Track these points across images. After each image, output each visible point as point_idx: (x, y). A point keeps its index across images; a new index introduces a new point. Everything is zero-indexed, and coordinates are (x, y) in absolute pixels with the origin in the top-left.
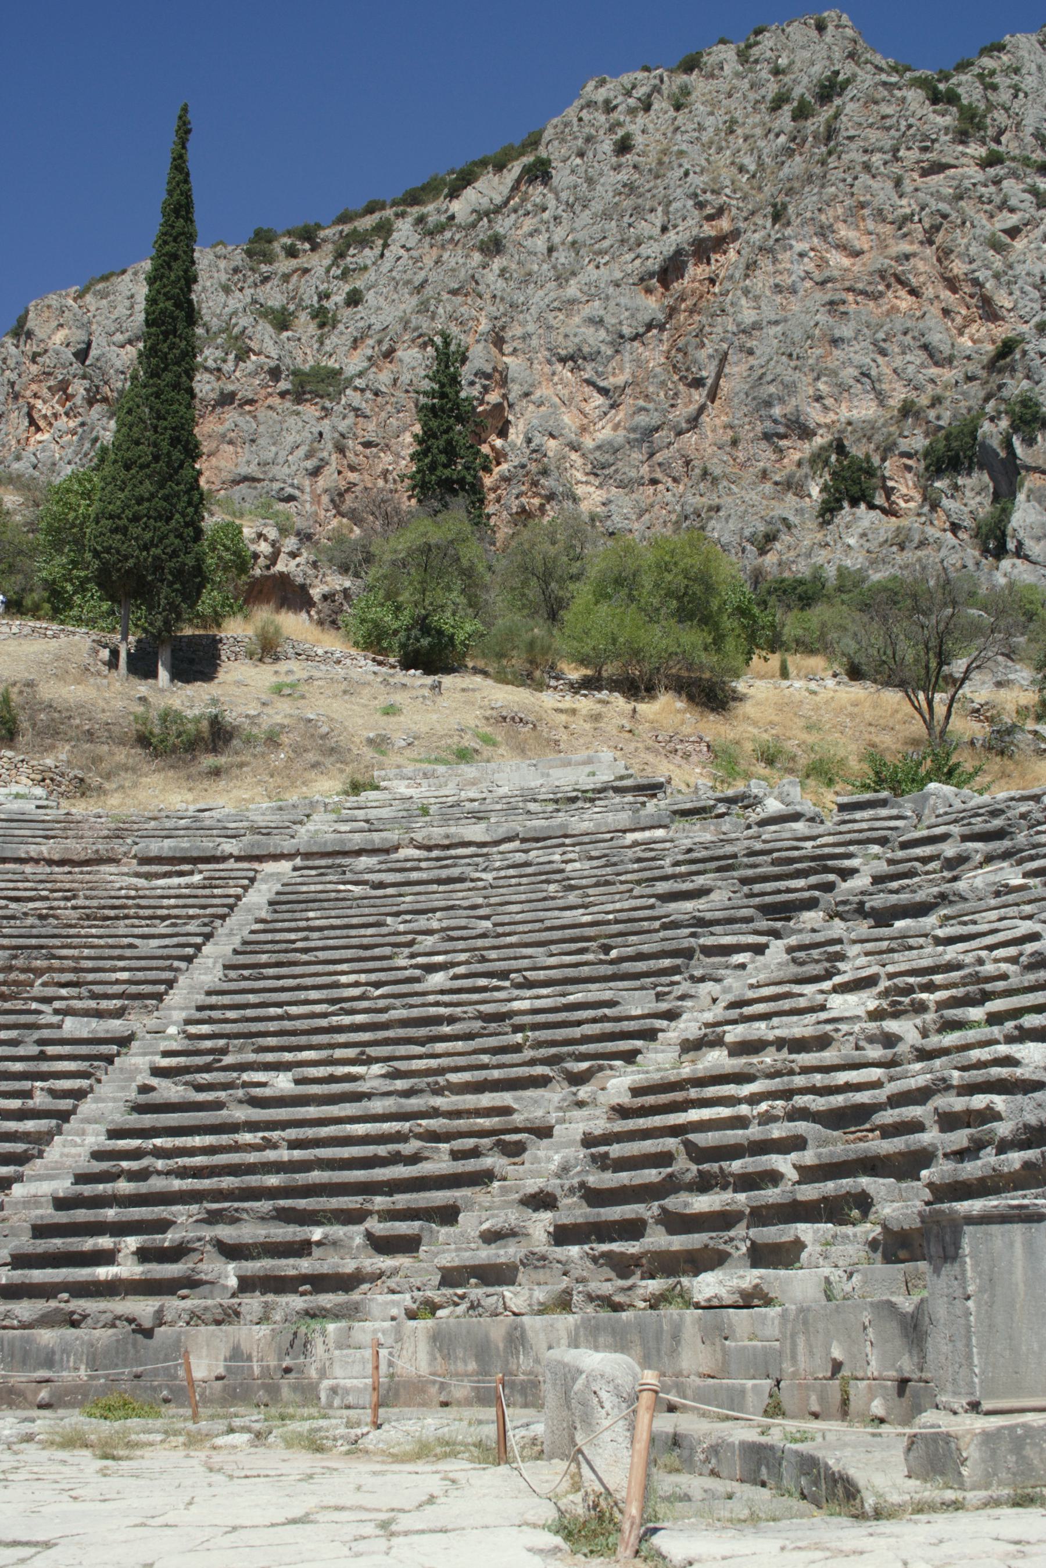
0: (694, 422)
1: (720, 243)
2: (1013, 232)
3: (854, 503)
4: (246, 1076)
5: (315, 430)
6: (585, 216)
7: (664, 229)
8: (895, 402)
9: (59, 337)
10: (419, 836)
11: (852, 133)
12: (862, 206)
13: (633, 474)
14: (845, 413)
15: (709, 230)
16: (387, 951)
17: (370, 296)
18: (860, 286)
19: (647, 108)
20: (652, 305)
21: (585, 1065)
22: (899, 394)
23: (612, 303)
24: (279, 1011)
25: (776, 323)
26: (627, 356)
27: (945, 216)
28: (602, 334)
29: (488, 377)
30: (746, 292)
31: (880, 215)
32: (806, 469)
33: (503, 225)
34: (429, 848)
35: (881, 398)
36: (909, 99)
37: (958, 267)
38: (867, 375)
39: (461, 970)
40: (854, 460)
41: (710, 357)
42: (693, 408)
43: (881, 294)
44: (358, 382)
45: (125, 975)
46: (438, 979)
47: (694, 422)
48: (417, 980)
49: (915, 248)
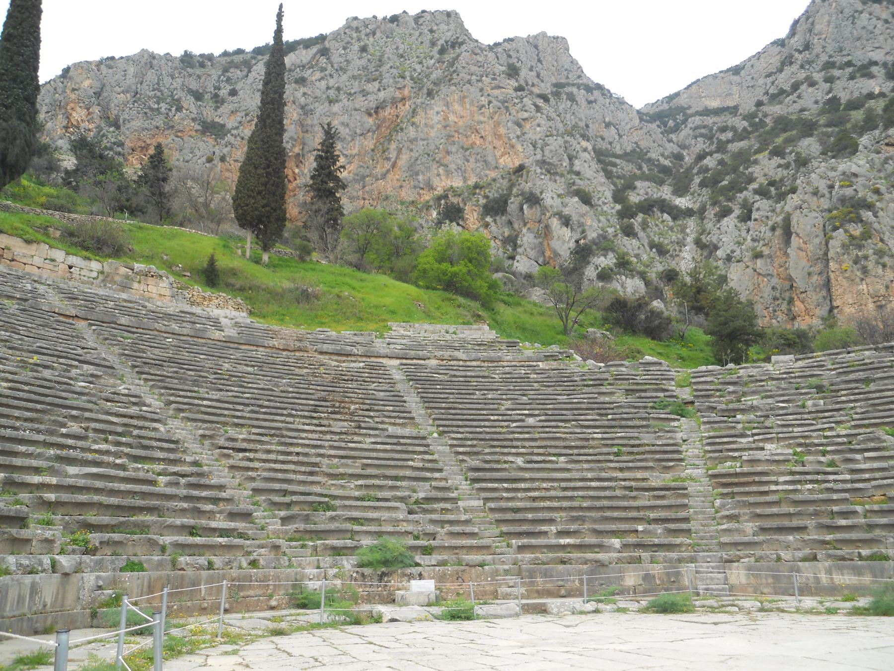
0: (384, 176)
3: (451, 221)
4: (506, 458)
5: (212, 150)
6: (344, 77)
7: (379, 90)
9: (87, 83)
11: (464, 65)
12: (464, 97)
13: (355, 194)
14: (449, 183)
15: (398, 95)
17: (241, 93)
18: (461, 131)
19: (374, 34)
20: (370, 121)
21: (671, 464)
23: (353, 118)
25: (424, 140)
26: (357, 143)
28: (347, 130)
29: (295, 140)
30: (413, 124)
33: (307, 74)
34: (442, 360)
35: (465, 179)
37: (502, 130)
39: (543, 418)
42: (384, 170)
44: (234, 132)
45: (391, 408)
46: (531, 421)
47: (384, 176)
48: (523, 421)
49: (485, 119)
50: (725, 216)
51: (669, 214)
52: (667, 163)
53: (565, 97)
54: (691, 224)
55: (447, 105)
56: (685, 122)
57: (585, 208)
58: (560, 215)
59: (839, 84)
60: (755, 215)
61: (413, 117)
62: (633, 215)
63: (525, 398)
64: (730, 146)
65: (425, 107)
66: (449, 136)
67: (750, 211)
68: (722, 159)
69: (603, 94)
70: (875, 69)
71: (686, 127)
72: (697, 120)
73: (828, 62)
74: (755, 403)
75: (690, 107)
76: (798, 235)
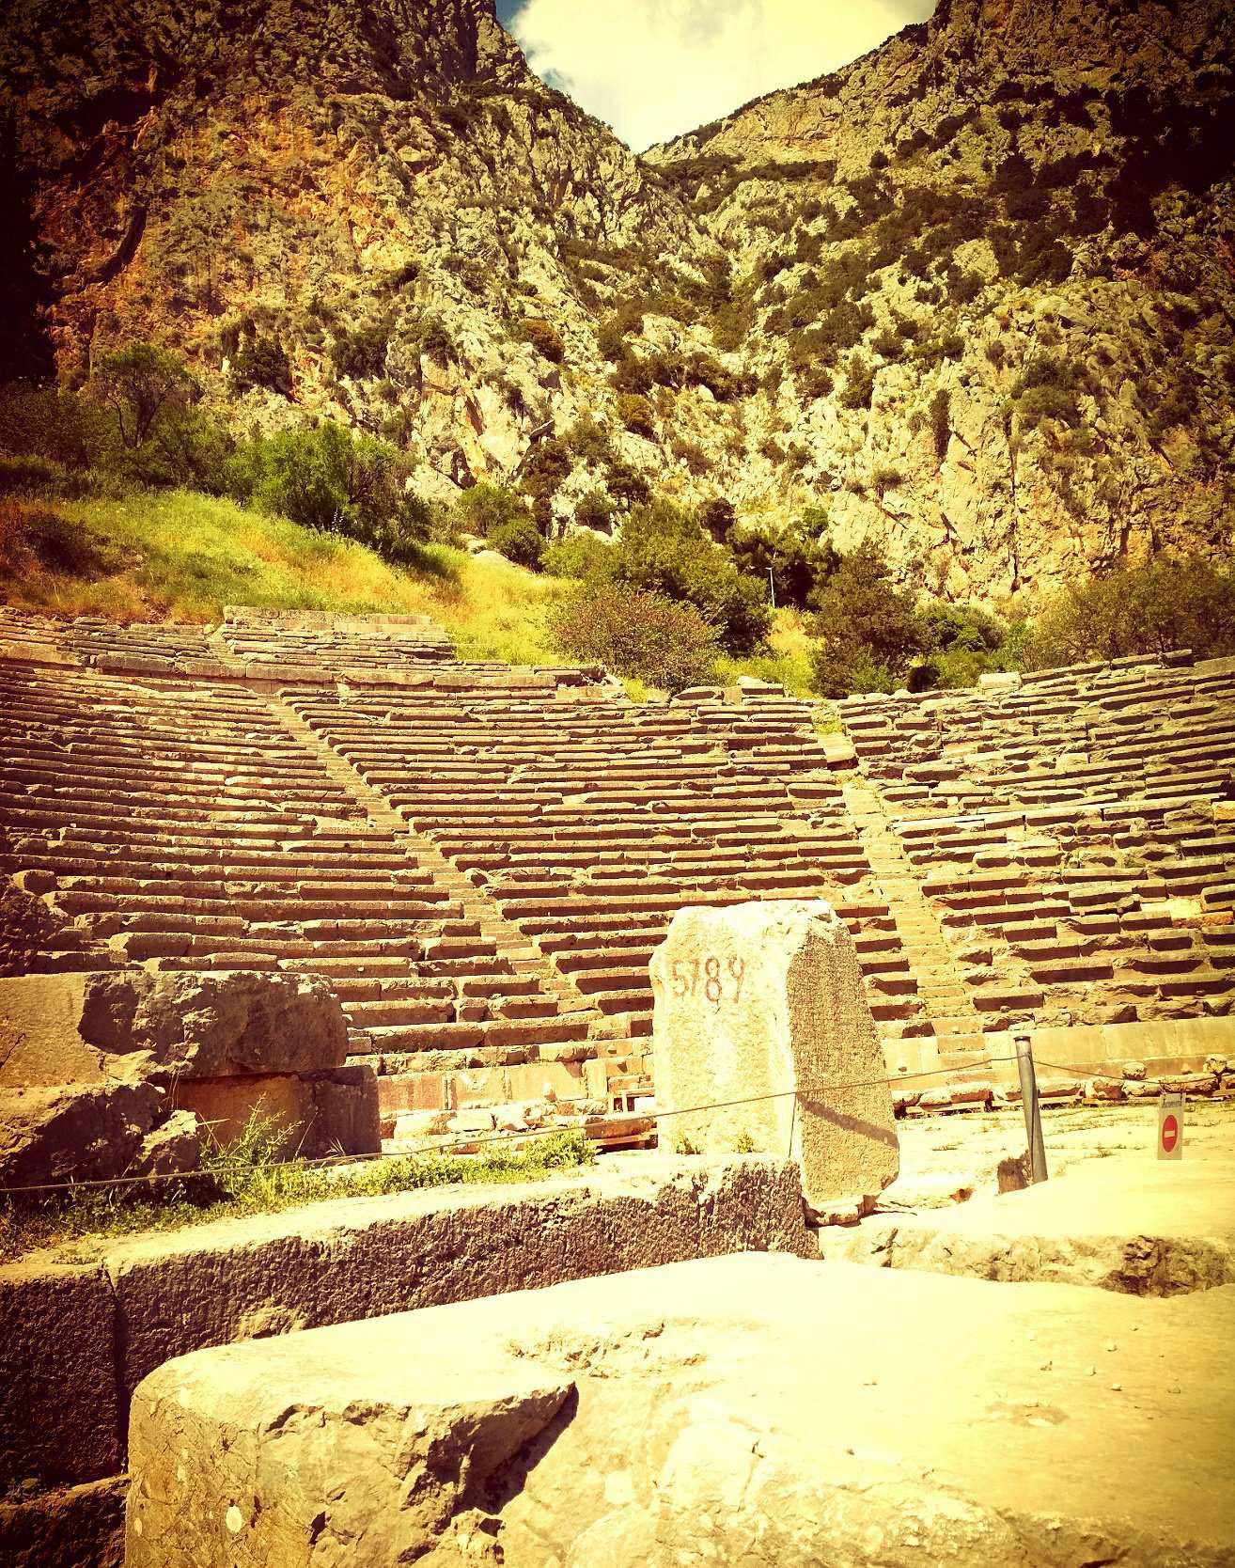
1: (145, 102)
2: (417, 167)
3: (263, 382)
4: (553, 870)
8: (305, 299)
10: (354, 673)
11: (278, 29)
14: (252, 299)
16: (501, 775)
18: (276, 180)
21: (852, 870)
22: (307, 294)
24: (491, 820)
25: (191, 195)
27: (359, 135)
31: (297, 118)
32: (216, 342)
35: (291, 293)
36: (332, 15)
38: (278, 267)
39: (595, 795)
40: (264, 342)
41: (126, 212)
42: (105, 259)
43: (296, 194)
46: (573, 802)
48: (559, 801)
49: (328, 157)
50: (818, 395)
51: (713, 388)
52: (697, 276)
53: (489, 120)
54: (754, 408)
55: (242, 118)
56: (730, 189)
57: (546, 367)
58: (495, 378)
59: (1027, 134)
60: (878, 396)
61: (167, 142)
62: (642, 387)
63: (547, 758)
64: (824, 246)
65: (192, 121)
66: (248, 192)
67: (868, 388)
68: (811, 275)
69: (569, 120)
70: (1093, 108)
71: (733, 200)
72: (755, 189)
73: (1006, 84)
74: (969, 760)
75: (740, 159)
76: (960, 438)
